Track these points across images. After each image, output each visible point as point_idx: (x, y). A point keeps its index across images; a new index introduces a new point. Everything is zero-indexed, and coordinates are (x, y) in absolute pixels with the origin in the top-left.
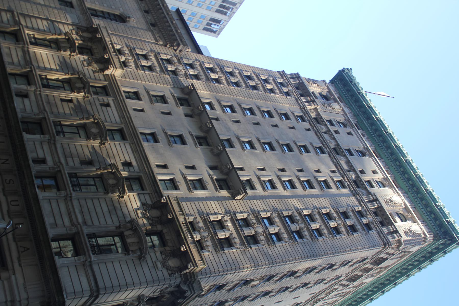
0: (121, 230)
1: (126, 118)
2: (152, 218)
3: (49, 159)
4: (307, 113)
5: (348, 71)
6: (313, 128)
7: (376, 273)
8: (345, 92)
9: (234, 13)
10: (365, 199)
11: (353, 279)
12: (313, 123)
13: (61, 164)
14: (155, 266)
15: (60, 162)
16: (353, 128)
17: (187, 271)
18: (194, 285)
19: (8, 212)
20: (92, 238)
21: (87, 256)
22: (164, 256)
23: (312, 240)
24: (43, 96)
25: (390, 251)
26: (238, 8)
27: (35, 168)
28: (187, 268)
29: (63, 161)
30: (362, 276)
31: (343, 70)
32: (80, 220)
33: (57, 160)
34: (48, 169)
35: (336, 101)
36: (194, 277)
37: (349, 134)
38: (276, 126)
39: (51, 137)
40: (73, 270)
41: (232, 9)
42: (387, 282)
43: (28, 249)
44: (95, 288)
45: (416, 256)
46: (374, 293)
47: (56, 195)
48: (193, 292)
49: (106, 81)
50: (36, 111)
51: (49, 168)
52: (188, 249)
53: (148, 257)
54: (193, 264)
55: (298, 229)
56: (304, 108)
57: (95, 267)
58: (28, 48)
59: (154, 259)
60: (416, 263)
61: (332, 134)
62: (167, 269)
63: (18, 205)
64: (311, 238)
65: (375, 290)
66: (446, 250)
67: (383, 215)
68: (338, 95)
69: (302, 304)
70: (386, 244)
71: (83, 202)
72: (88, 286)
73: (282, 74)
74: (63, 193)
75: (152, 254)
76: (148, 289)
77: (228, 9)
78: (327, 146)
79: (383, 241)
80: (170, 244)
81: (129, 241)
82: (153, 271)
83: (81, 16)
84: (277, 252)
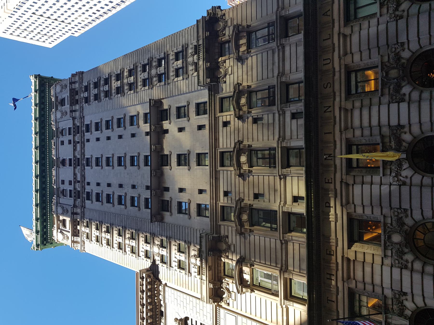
6: (84, 184)
15: (279, 115)
16: (58, 188)
19: (334, 51)
21: (278, 15)
23: (124, 69)
33: (281, 117)
34: (291, 105)
43: (323, 15)
47: (291, 77)
49: (220, 225)
52: (204, 33)
56: (82, 206)
63: (324, 60)
67: (73, 99)
74: (284, 79)
79: (82, 75)
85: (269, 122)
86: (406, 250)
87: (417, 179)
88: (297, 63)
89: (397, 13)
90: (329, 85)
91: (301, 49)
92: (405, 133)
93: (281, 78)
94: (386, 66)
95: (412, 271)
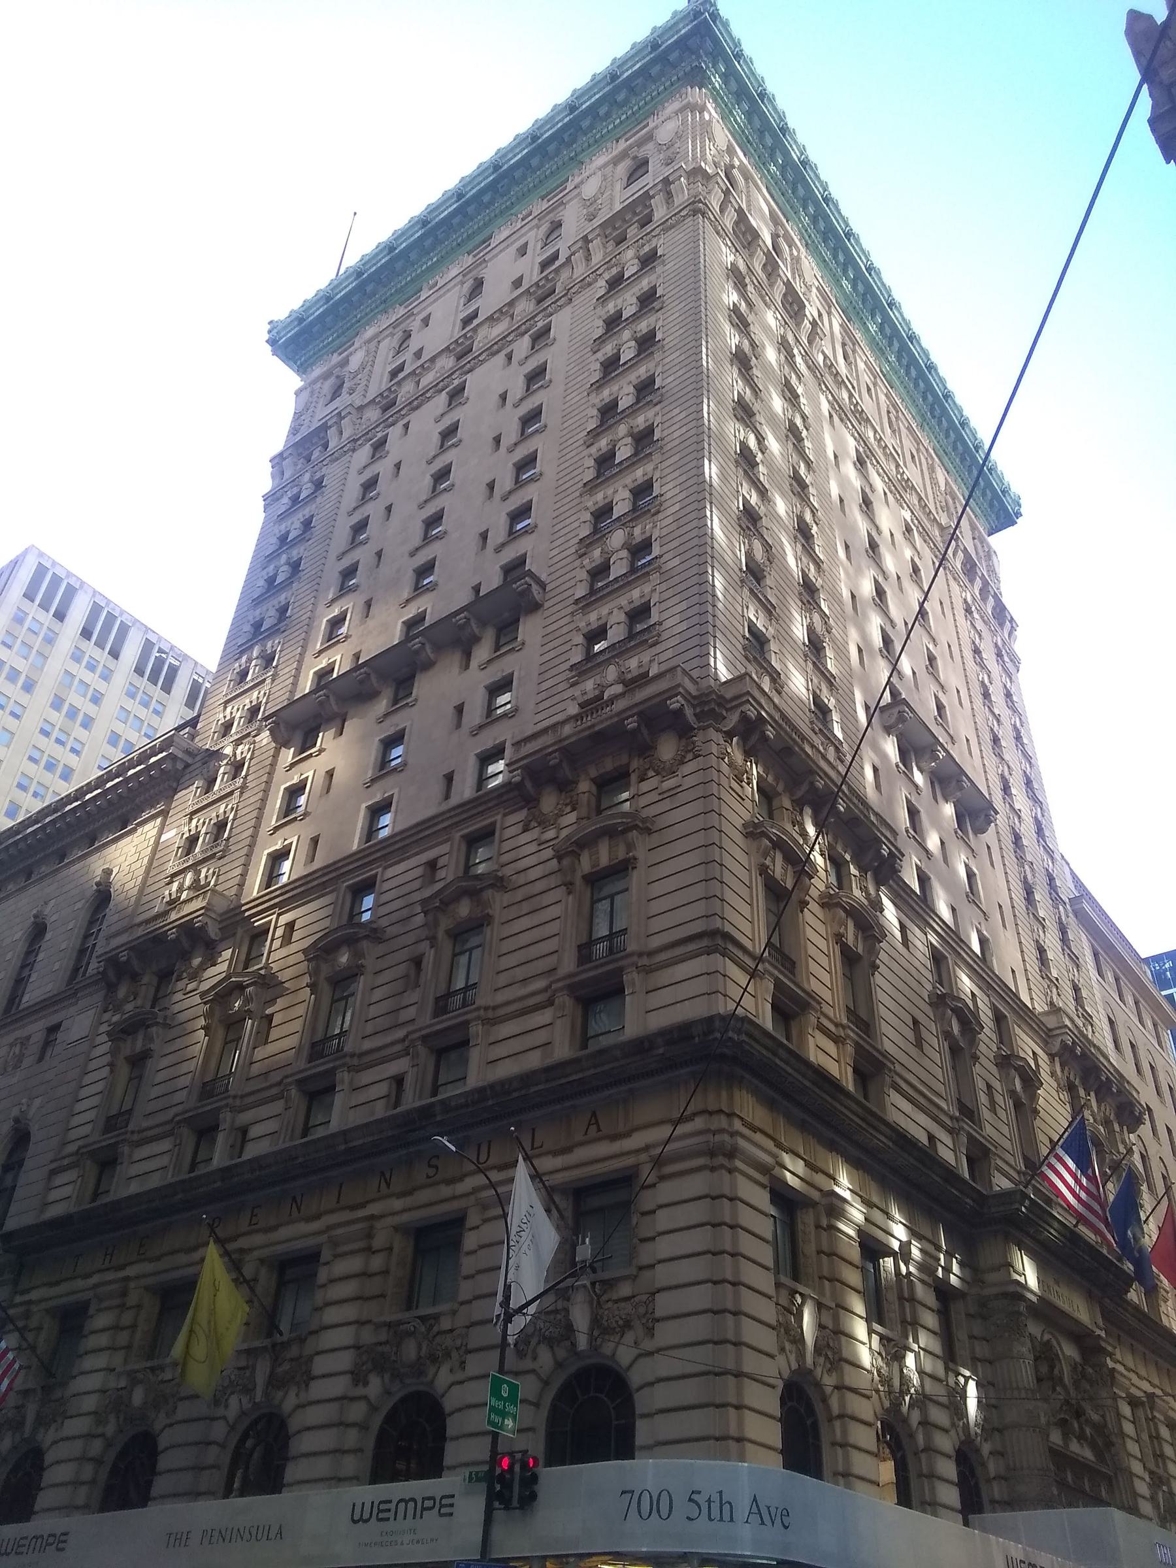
0: (578, 881)
1: (324, 879)
2: (560, 806)
3: (394, 1068)
4: (367, 433)
5: (276, 331)
7: (791, 250)
8: (328, 338)
9: (172, 648)
10: (580, 270)
11: (793, 306)
12: (391, 416)
13: (407, 1036)
14: (672, 793)
15: (403, 1040)
16: (413, 314)
17: (689, 712)
18: (728, 696)
20: (591, 954)
22: (651, 773)
24: (248, 1090)
25: (715, 202)
26: (160, 638)
27: (411, 1101)
28: (679, 712)
29: (400, 1033)
30: (788, 284)
31: (272, 342)
32: (540, 984)
33: (399, 1047)
34: (415, 1069)
35: (345, 362)
36: (707, 695)
37: (426, 322)
38: (389, 509)
39: (343, 1065)
40: (657, 999)
41: (160, 651)
42: (822, 225)
44: (705, 942)
45: (747, 138)
46: (849, 262)
47: (479, 1047)
48: (744, 699)
49: (234, 934)
50: (278, 1107)
51: (413, 1066)
53: (645, 813)
54: (670, 698)
55: (629, 440)
56: (355, 441)
57: (656, 942)
58: (133, 1132)
59: (654, 797)
60: (769, 141)
61: (422, 366)
62: (682, 763)
63: (490, 1142)
64: (656, 405)
65: (841, 258)
66: (732, 52)
68: (335, 355)
69: (861, 450)
70: (697, 208)
71: (503, 979)
72: (698, 959)
73: (270, 499)
75: (643, 801)
76: (725, 811)
77: (160, 662)
78: (447, 377)
80: (624, 759)
81: (604, 860)
82: (683, 797)
83: (82, 1003)
84: (677, 490)
85: (401, 1011)
86: (121, 1419)
87: (219, 1431)
88: (507, 1060)
89: (534, 1341)
90: (431, 1172)
91: (534, 1061)
92: (297, 1395)
93: (478, 1018)
94: (432, 1326)
95: (90, 1436)
